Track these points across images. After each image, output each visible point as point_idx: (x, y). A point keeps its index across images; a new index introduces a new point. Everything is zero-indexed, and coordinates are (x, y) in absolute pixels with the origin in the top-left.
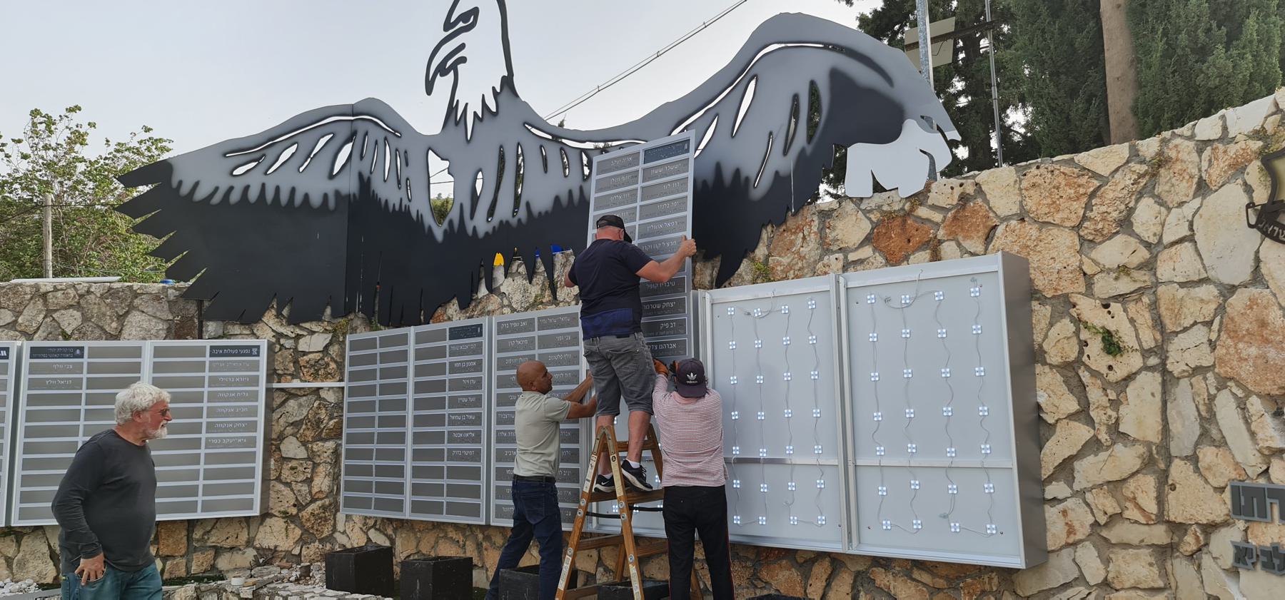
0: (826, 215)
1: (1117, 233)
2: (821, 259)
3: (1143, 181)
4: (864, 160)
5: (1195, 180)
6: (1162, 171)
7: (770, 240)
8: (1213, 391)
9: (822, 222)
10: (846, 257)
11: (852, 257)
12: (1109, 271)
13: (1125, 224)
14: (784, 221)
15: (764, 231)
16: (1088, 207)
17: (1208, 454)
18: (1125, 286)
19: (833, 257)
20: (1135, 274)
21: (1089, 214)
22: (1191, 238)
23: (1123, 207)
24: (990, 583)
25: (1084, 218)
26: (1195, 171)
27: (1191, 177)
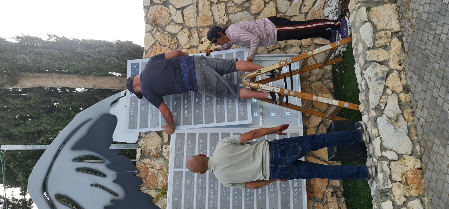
0: (142, 157)
1: (177, 38)
2: (164, 157)
3: (160, 29)
4: (123, 135)
5: (164, 7)
6: (158, 22)
7: (148, 188)
8: (233, 4)
9: (146, 158)
10: (166, 144)
11: (166, 140)
12: (190, 40)
13: (174, 35)
14: (141, 178)
15: (143, 192)
16: (165, 46)
17: (254, 8)
18: (196, 36)
19: (165, 150)
20: (192, 32)
21: (168, 46)
22: (182, 9)
23: (168, 35)
24: (306, 85)
25: (169, 47)
26: (160, 6)
27: (162, 9)
